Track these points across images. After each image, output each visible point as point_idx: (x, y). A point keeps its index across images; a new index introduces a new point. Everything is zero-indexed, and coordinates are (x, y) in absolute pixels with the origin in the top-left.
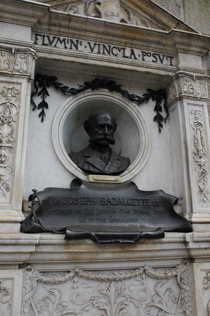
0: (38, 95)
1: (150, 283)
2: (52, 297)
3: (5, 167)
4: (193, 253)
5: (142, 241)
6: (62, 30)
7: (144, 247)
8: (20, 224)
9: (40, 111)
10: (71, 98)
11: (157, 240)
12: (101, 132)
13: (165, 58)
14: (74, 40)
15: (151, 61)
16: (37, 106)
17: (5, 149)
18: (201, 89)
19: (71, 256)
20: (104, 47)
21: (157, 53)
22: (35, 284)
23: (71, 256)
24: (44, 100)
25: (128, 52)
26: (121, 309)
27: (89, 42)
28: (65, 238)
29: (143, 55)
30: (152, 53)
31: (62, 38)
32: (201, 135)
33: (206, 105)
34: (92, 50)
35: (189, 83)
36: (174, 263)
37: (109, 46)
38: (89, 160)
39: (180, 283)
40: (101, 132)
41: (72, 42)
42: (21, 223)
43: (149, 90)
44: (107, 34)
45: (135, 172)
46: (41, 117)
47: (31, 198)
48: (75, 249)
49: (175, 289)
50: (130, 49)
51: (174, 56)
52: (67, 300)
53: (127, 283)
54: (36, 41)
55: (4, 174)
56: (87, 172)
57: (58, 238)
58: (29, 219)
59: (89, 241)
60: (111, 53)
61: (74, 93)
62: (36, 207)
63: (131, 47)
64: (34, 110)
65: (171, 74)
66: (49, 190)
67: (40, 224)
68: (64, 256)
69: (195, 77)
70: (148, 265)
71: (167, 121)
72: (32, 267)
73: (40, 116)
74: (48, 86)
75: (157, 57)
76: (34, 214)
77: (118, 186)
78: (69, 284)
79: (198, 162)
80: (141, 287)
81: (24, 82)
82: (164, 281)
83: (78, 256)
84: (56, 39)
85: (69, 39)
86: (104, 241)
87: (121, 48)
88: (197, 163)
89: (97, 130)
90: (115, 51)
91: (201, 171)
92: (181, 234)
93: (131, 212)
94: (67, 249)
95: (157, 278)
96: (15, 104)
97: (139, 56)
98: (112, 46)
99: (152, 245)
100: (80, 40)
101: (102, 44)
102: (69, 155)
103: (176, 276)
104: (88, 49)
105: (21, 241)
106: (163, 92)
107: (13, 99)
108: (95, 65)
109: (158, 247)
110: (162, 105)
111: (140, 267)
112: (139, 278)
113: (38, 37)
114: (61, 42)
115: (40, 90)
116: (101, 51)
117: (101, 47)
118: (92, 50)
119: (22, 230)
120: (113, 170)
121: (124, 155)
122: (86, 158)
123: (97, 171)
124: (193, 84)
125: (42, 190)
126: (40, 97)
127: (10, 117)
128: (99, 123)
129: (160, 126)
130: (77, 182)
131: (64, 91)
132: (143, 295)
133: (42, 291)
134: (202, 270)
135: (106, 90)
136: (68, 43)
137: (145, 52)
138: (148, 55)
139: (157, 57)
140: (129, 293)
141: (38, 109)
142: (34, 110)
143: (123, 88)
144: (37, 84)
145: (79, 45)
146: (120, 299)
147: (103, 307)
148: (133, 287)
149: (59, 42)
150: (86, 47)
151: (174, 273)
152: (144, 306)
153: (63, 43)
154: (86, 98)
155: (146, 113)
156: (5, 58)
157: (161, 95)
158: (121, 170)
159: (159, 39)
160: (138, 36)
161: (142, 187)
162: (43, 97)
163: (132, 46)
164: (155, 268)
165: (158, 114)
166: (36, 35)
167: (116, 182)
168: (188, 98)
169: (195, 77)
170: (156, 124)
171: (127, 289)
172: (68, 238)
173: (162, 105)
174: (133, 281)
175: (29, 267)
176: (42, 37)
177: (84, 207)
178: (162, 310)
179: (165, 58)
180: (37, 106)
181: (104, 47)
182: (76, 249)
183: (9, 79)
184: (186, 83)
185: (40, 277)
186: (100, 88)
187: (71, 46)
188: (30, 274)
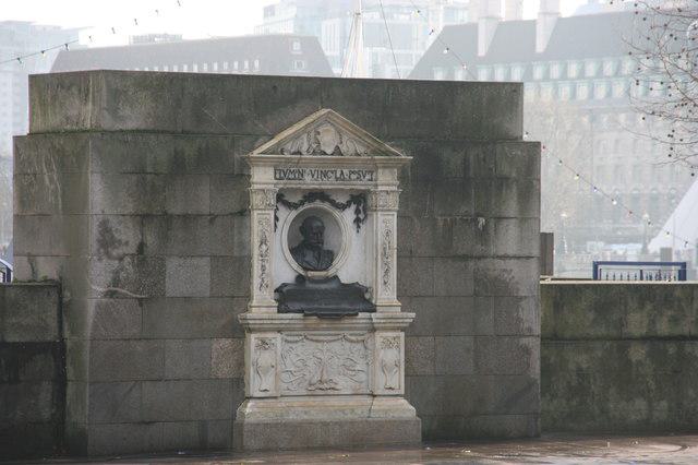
1: (348, 345)
4: (376, 325)
33: (396, 214)
49: (363, 348)
57: (300, 316)
70: (346, 333)
77: (327, 280)
92: (368, 314)
95: (352, 341)
109: (354, 321)
110: (361, 208)
120: (324, 267)
129: (359, 227)
130: (300, 279)
132: (343, 352)
148: (336, 346)
155: (349, 216)
157: (361, 202)
161: (345, 278)
164: (351, 335)
172: (305, 315)
173: (361, 208)
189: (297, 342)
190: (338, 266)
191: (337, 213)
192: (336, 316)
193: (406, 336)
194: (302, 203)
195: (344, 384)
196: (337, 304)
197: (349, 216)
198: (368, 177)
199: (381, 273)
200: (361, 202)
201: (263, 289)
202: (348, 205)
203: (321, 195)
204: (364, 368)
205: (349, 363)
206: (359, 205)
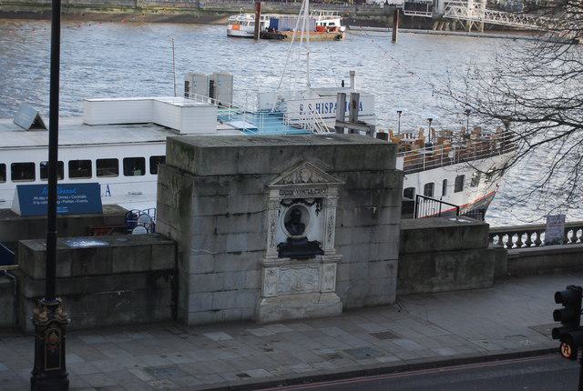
61: (288, 206)
102: (286, 225)
121: (304, 222)
130: (289, 239)
155: (314, 208)
157: (319, 202)
161: (310, 239)
194: (292, 204)
197: (314, 208)
199: (327, 236)
200: (319, 202)
202: (313, 204)
203: (302, 200)
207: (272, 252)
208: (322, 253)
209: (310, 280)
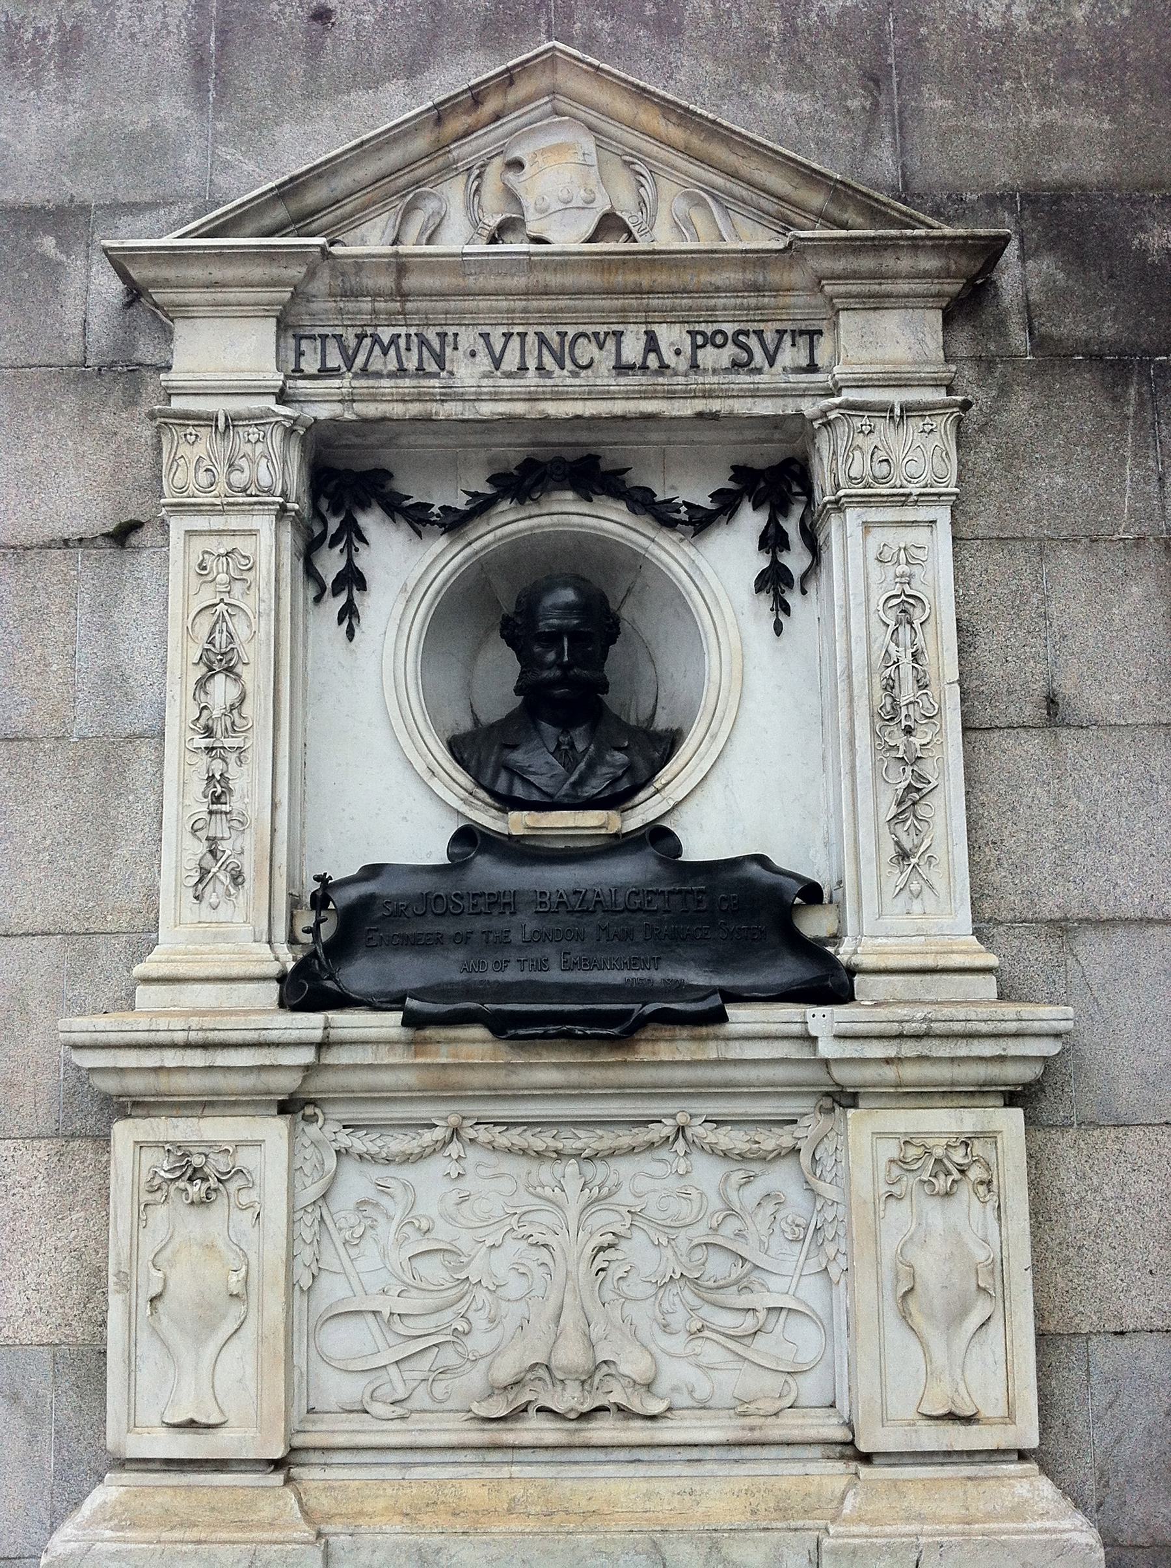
0: (332, 546)
2: (384, 1201)
3: (226, 813)
4: (842, 1074)
5: (648, 1033)
6: (381, 305)
7: (665, 1052)
8: (275, 987)
9: (342, 599)
10: (442, 542)
11: (704, 1031)
12: (551, 656)
13: (787, 339)
14: (431, 334)
15: (726, 363)
16: (329, 582)
17: (224, 760)
18: (923, 454)
19: (429, 1077)
20: (542, 340)
21: (751, 327)
22: (331, 1162)
23: (429, 1077)
24: (350, 561)
25: (632, 350)
26: (602, 1249)
27: (487, 329)
28: (405, 1023)
29: (696, 347)
30: (730, 329)
31: (385, 334)
32: (913, 644)
33: (943, 515)
34: (497, 362)
35: (874, 439)
36: (789, 1107)
37: (562, 335)
38: (518, 757)
39: (810, 1177)
40: (551, 656)
41: (423, 342)
42: (281, 979)
43: (740, 472)
44: (546, 292)
45: (676, 792)
46: (346, 624)
47: (319, 902)
48: (437, 1054)
49: (795, 1195)
50: (643, 328)
51: (824, 325)
52: (433, 1212)
53: (624, 1167)
54: (298, 363)
55: (226, 835)
56: (507, 803)
57: (389, 1022)
58: (302, 967)
59: (478, 1032)
60: (568, 362)
61: (454, 523)
62: (327, 931)
63: (646, 323)
64: (318, 600)
65: (809, 407)
66: (372, 872)
67: (336, 982)
68: (408, 1078)
69: (897, 411)
71: (811, 588)
72: (317, 1111)
73: (340, 621)
74: (364, 506)
75: (753, 342)
76: (320, 951)
78: (438, 1166)
79: (895, 748)
80: (673, 1183)
81: (264, 523)
82: (755, 1168)
83: (456, 1077)
84: (367, 341)
85: (413, 330)
86: (521, 1032)
87: (607, 334)
88: (894, 754)
89: (537, 649)
90: (586, 351)
91: (904, 784)
93: (639, 937)
94: (416, 1055)
96: (242, 606)
97: (678, 353)
98: (571, 331)
99: (693, 1046)
100: (451, 330)
101: (531, 330)
102: (457, 747)
103: (795, 1151)
104: (484, 362)
105: (274, 1036)
106: (796, 468)
107: (238, 587)
108: (510, 420)
109: (712, 1051)
110: (791, 526)
111: (666, 1116)
112: (664, 1153)
113: (305, 345)
114: (385, 353)
115: (334, 524)
116: (532, 364)
117: (531, 339)
118: (497, 362)
119: (284, 1004)
122: (506, 751)
123: (536, 797)
124: (891, 432)
125: (354, 871)
126: (341, 546)
127: (233, 649)
128: (543, 627)
130: (468, 838)
131: (417, 518)
133: (356, 1183)
134: (879, 1135)
135: (570, 495)
136: (408, 349)
137: (702, 333)
138: (709, 340)
139: (753, 342)
140: (631, 1200)
141: (335, 594)
142: (318, 600)
143: (636, 478)
144: (324, 504)
145: (448, 350)
146: (601, 1219)
147: (542, 1239)
148: (643, 1181)
149: (377, 350)
150: (473, 354)
151: (787, 1142)
152: (683, 1246)
153: (392, 352)
154: (499, 532)
156: (201, 449)
158: (625, 784)
159: (749, 276)
160: (663, 278)
161: (701, 843)
162: (350, 551)
163: (648, 317)
165: (775, 562)
166: (299, 338)
167: (603, 832)
168: (866, 501)
169: (897, 411)
170: (765, 602)
171: (625, 1188)
172: (412, 1021)
174: (645, 1164)
175: (309, 1111)
176: (318, 343)
177: (479, 924)
178: (744, 1260)
179: (787, 339)
180: (329, 582)
181: (542, 340)
182: (443, 1055)
183: (217, 522)
184: (860, 440)
185: (344, 1139)
186: (546, 491)
187: (421, 360)
188: (313, 1130)
189: (408, 1159)
190: (676, 792)
191: (668, 552)
192: (611, 1027)
193: (1031, 1122)
194: (481, 506)
195: (694, 1373)
196: (635, 963)
197: (727, 561)
198: (790, 356)
200: (776, 483)
201: (211, 897)
202: (726, 506)
204: (811, 1292)
205: (718, 1267)
206: (780, 508)
207: (220, 950)
208: (828, 982)
209: (714, 1283)
